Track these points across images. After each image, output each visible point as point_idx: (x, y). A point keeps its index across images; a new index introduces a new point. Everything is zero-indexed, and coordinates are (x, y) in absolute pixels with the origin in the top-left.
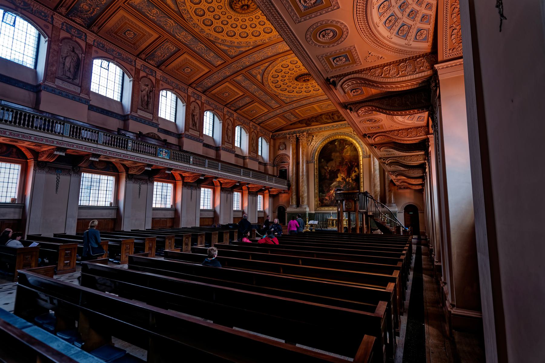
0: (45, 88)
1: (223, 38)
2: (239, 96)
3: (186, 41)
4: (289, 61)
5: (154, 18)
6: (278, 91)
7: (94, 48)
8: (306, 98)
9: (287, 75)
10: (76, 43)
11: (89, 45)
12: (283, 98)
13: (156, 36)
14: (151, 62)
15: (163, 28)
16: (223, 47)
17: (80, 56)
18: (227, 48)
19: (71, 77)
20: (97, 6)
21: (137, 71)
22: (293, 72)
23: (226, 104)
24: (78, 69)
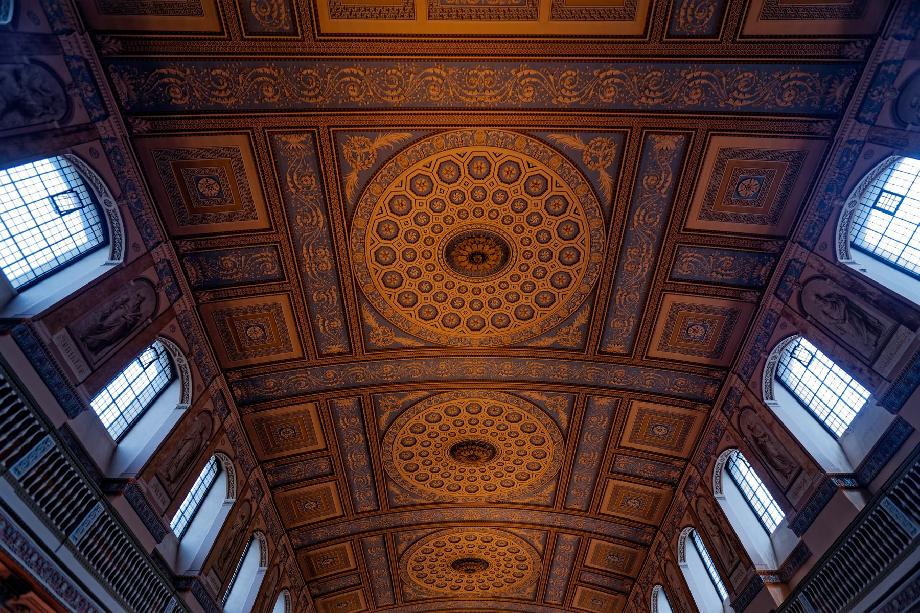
0: (129, 490)
1: (406, 478)
2: (351, 568)
3: (353, 467)
4: (465, 534)
5: (344, 427)
6: (411, 577)
7: (225, 436)
8: (446, 598)
9: (446, 554)
10: (211, 422)
11: (223, 430)
12: (409, 591)
13: (321, 445)
14: (270, 478)
15: (340, 440)
16: (395, 490)
17: (203, 444)
18: (398, 492)
19: (172, 478)
20: (287, 389)
21: (246, 487)
22: (458, 551)
23: (312, 579)
24: (187, 466)
